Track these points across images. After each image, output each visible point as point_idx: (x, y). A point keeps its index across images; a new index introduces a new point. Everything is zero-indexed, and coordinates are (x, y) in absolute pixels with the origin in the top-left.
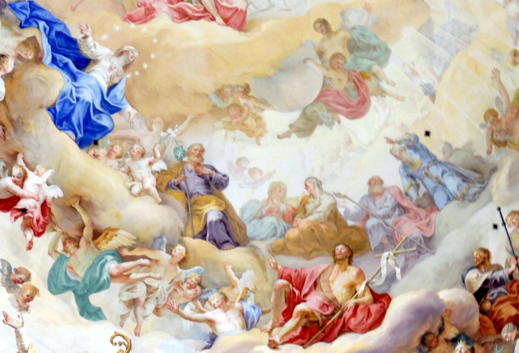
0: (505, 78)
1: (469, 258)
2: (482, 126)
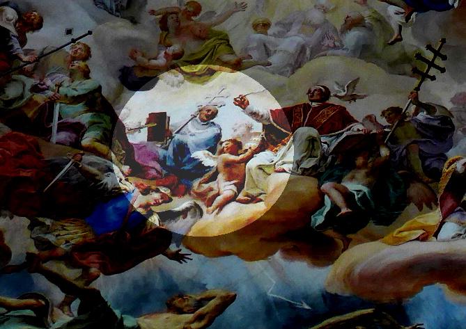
0: (238, 17)
1: (30, 8)
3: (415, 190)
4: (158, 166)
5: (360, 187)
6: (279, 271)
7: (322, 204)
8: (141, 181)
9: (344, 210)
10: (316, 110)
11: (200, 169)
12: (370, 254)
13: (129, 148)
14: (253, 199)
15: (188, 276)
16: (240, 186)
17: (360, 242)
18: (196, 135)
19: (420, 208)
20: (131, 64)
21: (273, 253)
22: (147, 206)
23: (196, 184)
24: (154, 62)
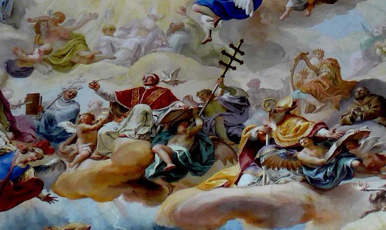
0: (92, 24)
2: (50, 12)
3: (221, 150)
4: (33, 133)
5: (181, 148)
6: (122, 210)
7: (153, 160)
8: (21, 143)
9: (170, 165)
10: (149, 92)
11: (65, 134)
12: (188, 196)
13: (12, 120)
14: (103, 157)
15: (55, 213)
16: (93, 148)
17: (181, 188)
18: (61, 110)
19: (225, 163)
20: (13, 58)
21: (118, 196)
22: (25, 162)
23: (61, 145)
24: (30, 57)
